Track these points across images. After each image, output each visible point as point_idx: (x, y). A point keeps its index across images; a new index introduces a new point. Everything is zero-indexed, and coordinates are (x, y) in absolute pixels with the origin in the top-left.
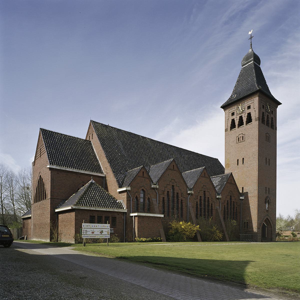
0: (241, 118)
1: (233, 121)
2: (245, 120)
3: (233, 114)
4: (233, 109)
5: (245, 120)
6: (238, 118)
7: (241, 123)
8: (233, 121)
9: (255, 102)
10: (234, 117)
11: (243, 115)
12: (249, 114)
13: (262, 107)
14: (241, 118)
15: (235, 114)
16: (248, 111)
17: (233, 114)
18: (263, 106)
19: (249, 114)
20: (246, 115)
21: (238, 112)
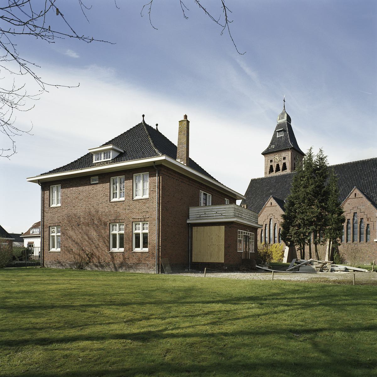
0: (278, 165)
1: (271, 167)
2: (281, 167)
3: (271, 161)
4: (271, 157)
5: (281, 167)
6: (276, 165)
7: (278, 169)
8: (271, 167)
9: (288, 155)
10: (272, 164)
11: (279, 163)
12: (284, 164)
13: (293, 159)
14: (278, 165)
15: (273, 161)
16: (284, 161)
17: (271, 161)
18: (295, 158)
19: (284, 164)
20: (283, 164)
21: (275, 160)
